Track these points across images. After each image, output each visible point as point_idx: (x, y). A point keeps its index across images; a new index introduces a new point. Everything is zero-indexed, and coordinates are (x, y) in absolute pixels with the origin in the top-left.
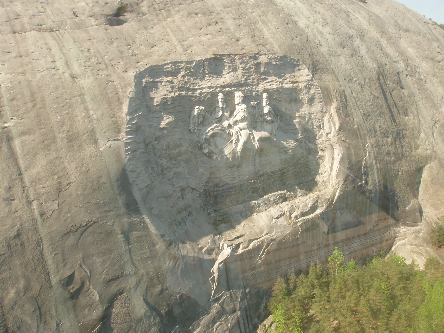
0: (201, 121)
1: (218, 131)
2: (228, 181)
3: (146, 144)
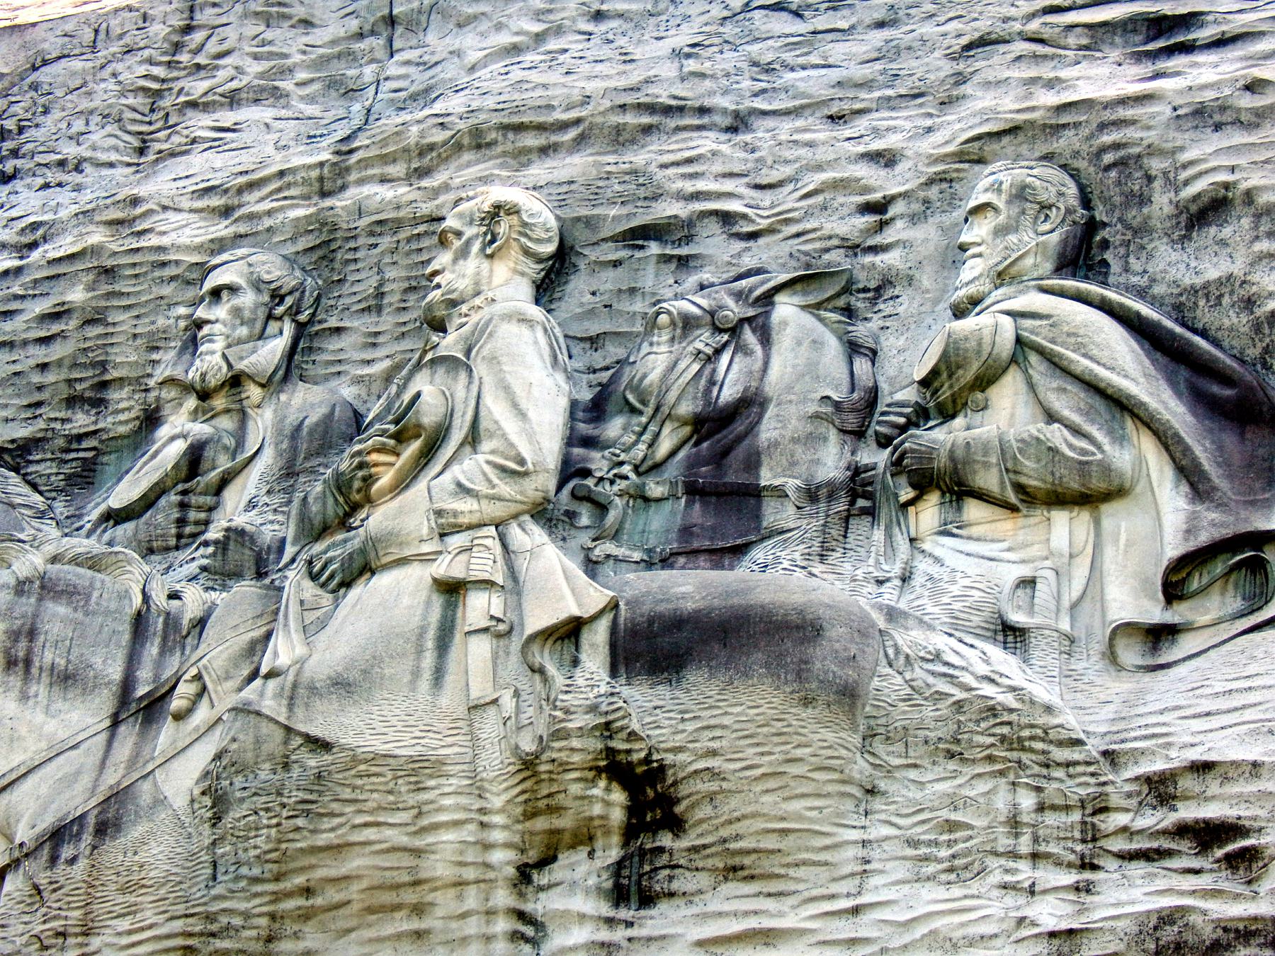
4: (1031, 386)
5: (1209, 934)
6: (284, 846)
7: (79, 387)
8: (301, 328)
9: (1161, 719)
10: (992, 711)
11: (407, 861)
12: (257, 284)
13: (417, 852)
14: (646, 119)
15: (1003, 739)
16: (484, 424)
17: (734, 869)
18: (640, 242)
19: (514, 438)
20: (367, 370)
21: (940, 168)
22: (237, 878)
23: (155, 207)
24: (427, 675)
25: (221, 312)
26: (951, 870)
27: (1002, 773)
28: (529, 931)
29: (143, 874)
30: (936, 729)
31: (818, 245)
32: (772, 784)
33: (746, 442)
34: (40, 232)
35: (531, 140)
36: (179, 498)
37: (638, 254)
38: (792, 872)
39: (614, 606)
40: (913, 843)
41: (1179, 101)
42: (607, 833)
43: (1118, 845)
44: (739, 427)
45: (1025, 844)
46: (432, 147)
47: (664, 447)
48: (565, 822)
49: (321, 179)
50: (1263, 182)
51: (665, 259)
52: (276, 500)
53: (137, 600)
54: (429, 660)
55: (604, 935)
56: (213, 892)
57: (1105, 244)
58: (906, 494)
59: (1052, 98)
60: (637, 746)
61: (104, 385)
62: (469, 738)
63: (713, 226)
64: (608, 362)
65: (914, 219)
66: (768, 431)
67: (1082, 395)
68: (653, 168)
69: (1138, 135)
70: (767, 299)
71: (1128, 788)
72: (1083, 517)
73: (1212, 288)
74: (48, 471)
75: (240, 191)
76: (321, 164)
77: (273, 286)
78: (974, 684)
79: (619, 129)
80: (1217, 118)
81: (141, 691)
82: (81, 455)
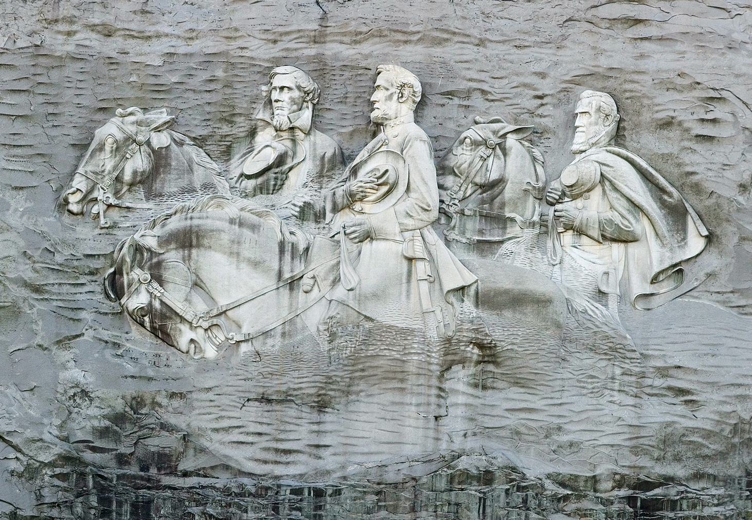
0: (135, 173)
1: (218, 224)
2: (242, 457)
4: (604, 191)
5: (682, 431)
6: (357, 355)
7: (225, 115)
8: (314, 105)
9: (659, 341)
10: (607, 337)
11: (399, 364)
12: (299, 88)
13: (404, 361)
14: (445, 36)
15: (610, 348)
16: (412, 186)
17: (517, 383)
18: (450, 97)
19: (426, 195)
20: (343, 130)
21: (565, 85)
22: (339, 364)
23: (245, 35)
24: (404, 293)
25: (286, 96)
26: (592, 393)
27: (609, 360)
28: (442, 394)
29: (302, 356)
30: (587, 340)
31: (519, 111)
32: (533, 357)
33: (500, 197)
34: (194, 34)
35: (400, 37)
36: (274, 175)
37: (450, 102)
38: (538, 387)
39: (476, 281)
40: (579, 381)
41: (655, 76)
42: (471, 362)
43: (648, 390)
44: (497, 190)
45: (616, 387)
46: (361, 33)
47: (469, 192)
48: (456, 358)
49: (315, 36)
50: (686, 118)
51: (460, 106)
52: (317, 186)
53: (280, 235)
54: (404, 286)
55: (471, 400)
56: (331, 368)
57: (624, 129)
58: (560, 229)
59: (604, 62)
60: (487, 338)
61: (234, 115)
62: (423, 322)
63: (477, 94)
64: (440, 148)
65: (554, 106)
66: (509, 192)
67: (626, 202)
68: (452, 63)
69: (640, 88)
70: (504, 136)
71: (651, 370)
72: (622, 245)
73: (665, 156)
74: (213, 149)
75: (281, 35)
76: (315, 31)
77: (306, 90)
78: (600, 326)
79: (434, 38)
80: (668, 86)
81: (287, 275)
82: (226, 143)
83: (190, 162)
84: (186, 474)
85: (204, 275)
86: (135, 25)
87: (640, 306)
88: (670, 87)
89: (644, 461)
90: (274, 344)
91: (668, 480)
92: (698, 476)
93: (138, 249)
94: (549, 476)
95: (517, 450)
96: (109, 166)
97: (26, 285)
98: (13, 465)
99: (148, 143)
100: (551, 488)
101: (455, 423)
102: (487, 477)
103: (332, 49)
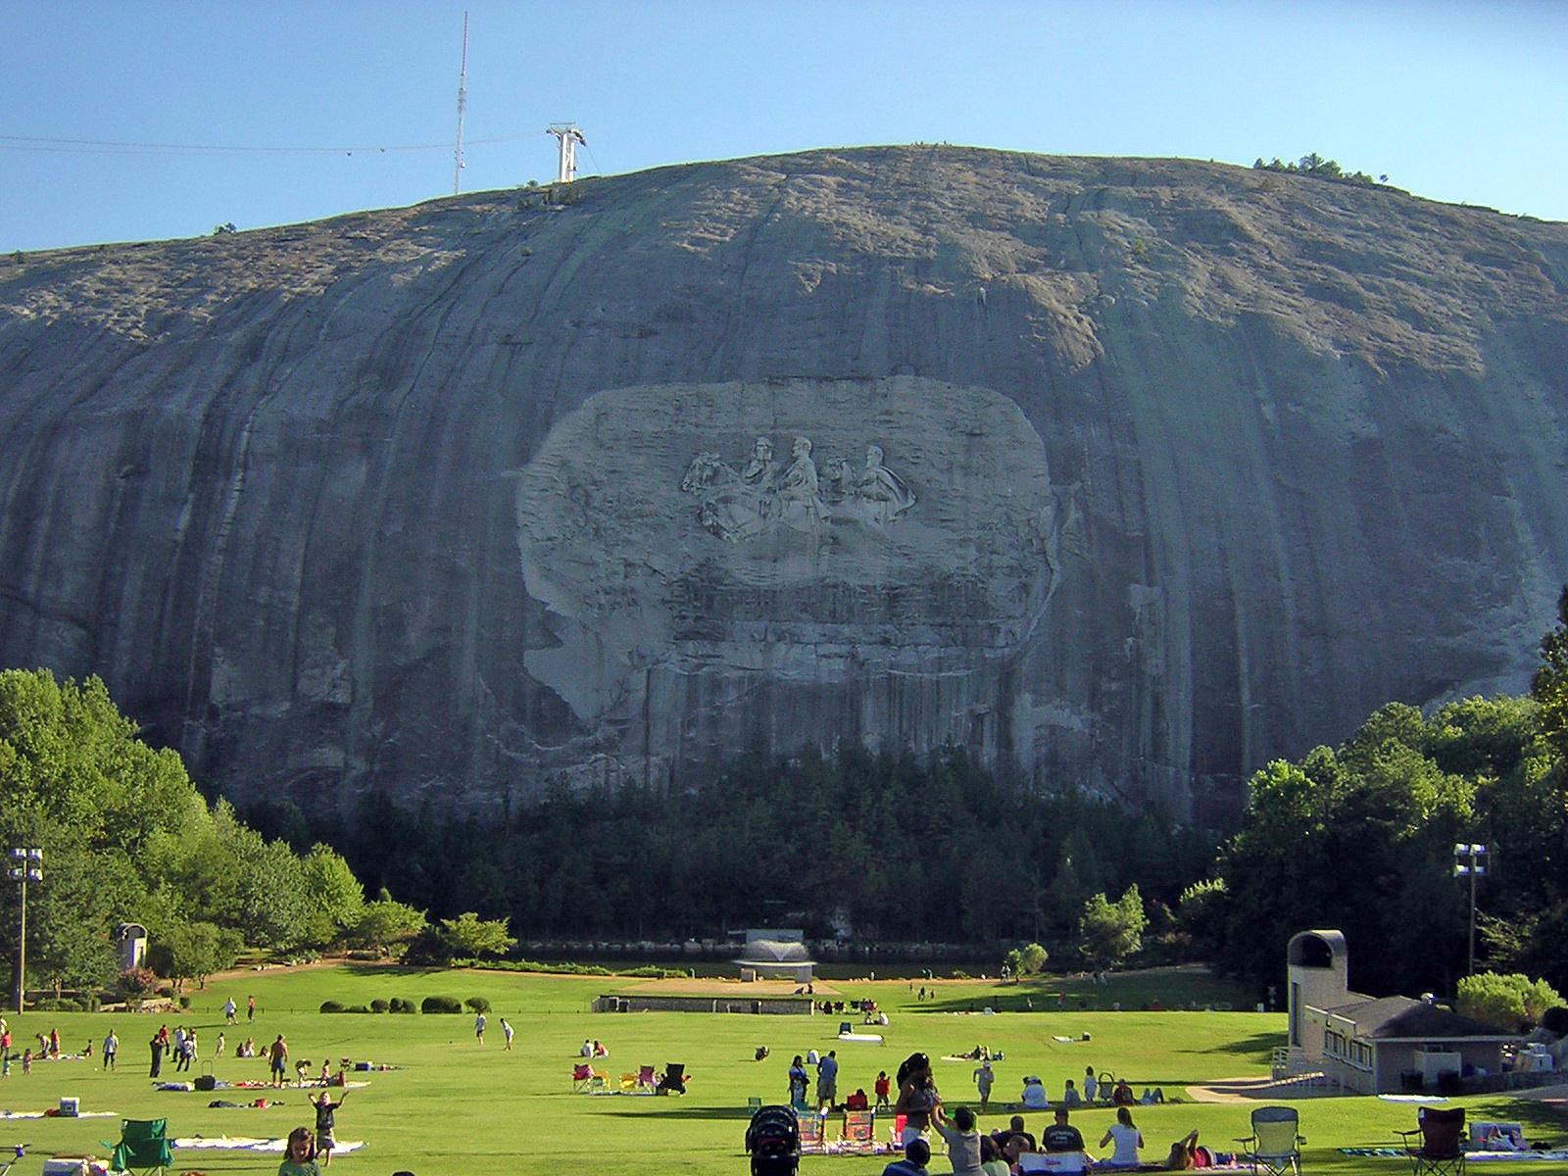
0: (707, 476)
2: (745, 578)
3: (572, 487)
25: (762, 448)
66: (843, 484)
83: (727, 472)
84: (726, 585)
85: (733, 514)
86: (708, 423)
87: (891, 523)
88: (901, 444)
89: (891, 580)
90: (757, 538)
91: (901, 587)
92: (913, 585)
93: (708, 504)
94: (859, 586)
95: (847, 575)
96: (698, 473)
97: (667, 516)
98: (662, 582)
99: (712, 465)
100: (859, 589)
101: (824, 567)
102: (835, 586)
103: (777, 432)
